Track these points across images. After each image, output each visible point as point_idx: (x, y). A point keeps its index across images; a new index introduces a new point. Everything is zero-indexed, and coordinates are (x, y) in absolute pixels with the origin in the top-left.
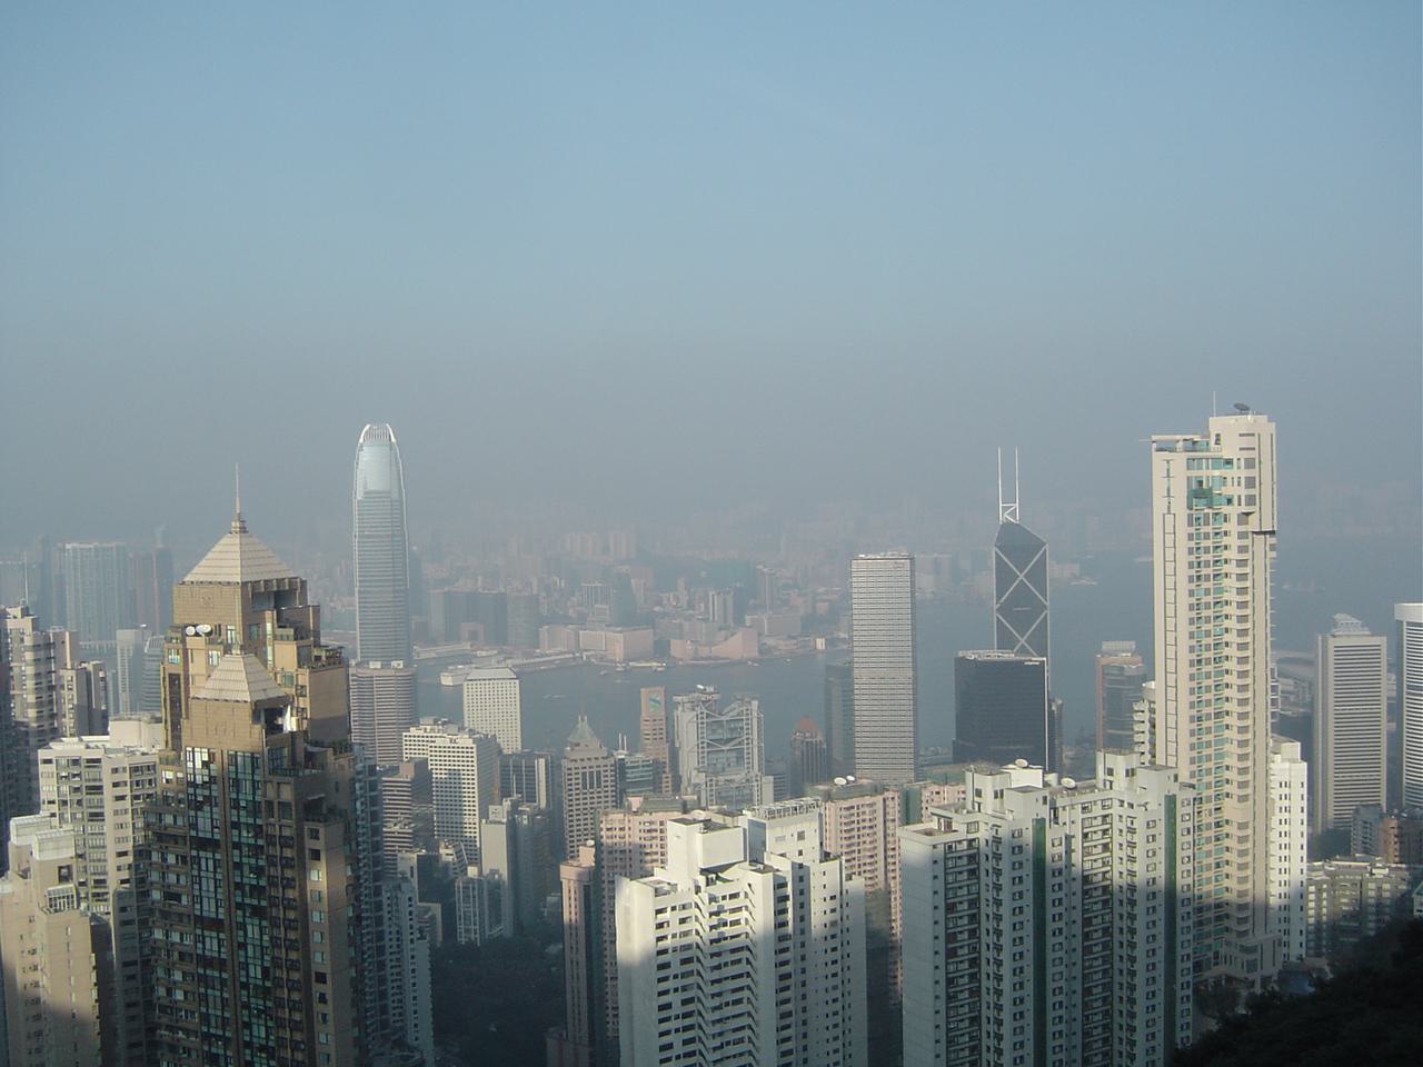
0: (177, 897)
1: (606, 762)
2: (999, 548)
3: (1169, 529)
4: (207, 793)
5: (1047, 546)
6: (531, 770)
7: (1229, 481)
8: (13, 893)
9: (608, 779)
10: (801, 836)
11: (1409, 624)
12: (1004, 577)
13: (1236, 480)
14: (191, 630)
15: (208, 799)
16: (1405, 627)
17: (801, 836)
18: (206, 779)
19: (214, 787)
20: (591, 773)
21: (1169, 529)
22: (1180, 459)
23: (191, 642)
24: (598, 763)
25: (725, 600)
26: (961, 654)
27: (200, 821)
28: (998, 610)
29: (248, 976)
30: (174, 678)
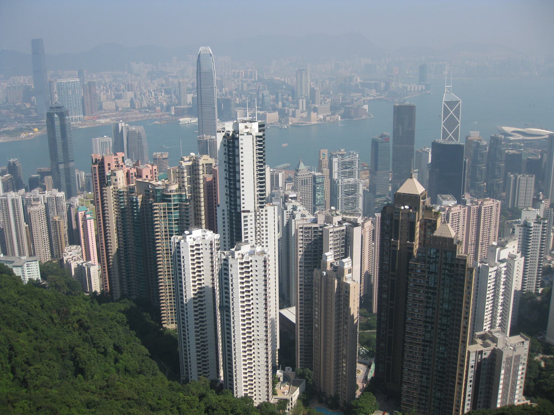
1: (309, 176)
2: (445, 102)
4: (434, 260)
5: (461, 102)
6: (277, 177)
9: (310, 182)
10: (514, 247)
12: (446, 112)
14: (402, 208)
17: (514, 247)
18: (434, 257)
19: (437, 259)
20: (304, 180)
24: (304, 177)
25: (303, 101)
26: (433, 141)
27: (431, 267)
28: (443, 124)
29: (443, 307)
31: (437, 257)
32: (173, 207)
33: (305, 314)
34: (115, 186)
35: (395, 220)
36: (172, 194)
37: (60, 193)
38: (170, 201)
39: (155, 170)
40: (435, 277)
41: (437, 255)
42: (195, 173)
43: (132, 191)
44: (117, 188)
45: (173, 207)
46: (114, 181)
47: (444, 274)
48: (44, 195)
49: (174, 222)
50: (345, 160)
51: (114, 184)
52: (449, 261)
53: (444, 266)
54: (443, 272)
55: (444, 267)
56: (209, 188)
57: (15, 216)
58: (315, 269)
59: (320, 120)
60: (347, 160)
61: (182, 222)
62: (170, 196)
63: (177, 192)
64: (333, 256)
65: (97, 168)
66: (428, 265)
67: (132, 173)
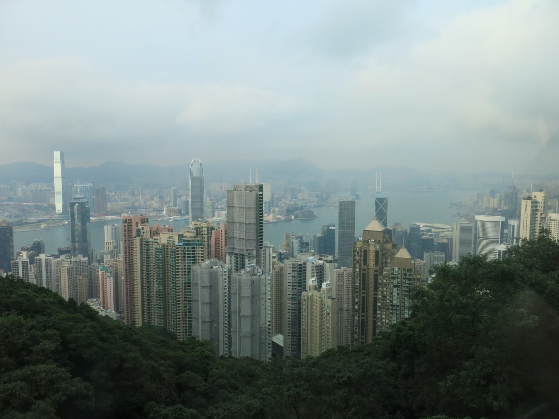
0: (386, 297)
3: (526, 216)
4: (397, 276)
7: (538, 206)
8: (313, 295)
11: (479, 221)
12: (377, 206)
13: (540, 207)
14: (370, 241)
15: (397, 278)
16: (478, 221)
18: (397, 273)
19: (399, 275)
21: (526, 216)
22: (529, 202)
23: (370, 243)
27: (394, 282)
30: (365, 251)
31: (399, 274)
32: (191, 250)
33: (292, 333)
34: (143, 237)
35: (364, 250)
36: (191, 239)
37: (84, 258)
38: (189, 244)
39: (172, 229)
40: (397, 289)
41: (399, 272)
42: (201, 233)
43: (156, 241)
44: (144, 239)
45: (191, 250)
46: (142, 234)
47: (404, 287)
48: (71, 259)
49: (191, 261)
50: (303, 242)
51: (142, 236)
52: (408, 277)
53: (404, 280)
54: (404, 285)
55: (404, 281)
56: (216, 240)
57: (47, 273)
58: (303, 292)
59: (279, 219)
60: (305, 241)
61: (198, 261)
62: (189, 241)
63: (195, 238)
64: (317, 281)
65: (127, 226)
66: (392, 280)
67: (154, 231)
